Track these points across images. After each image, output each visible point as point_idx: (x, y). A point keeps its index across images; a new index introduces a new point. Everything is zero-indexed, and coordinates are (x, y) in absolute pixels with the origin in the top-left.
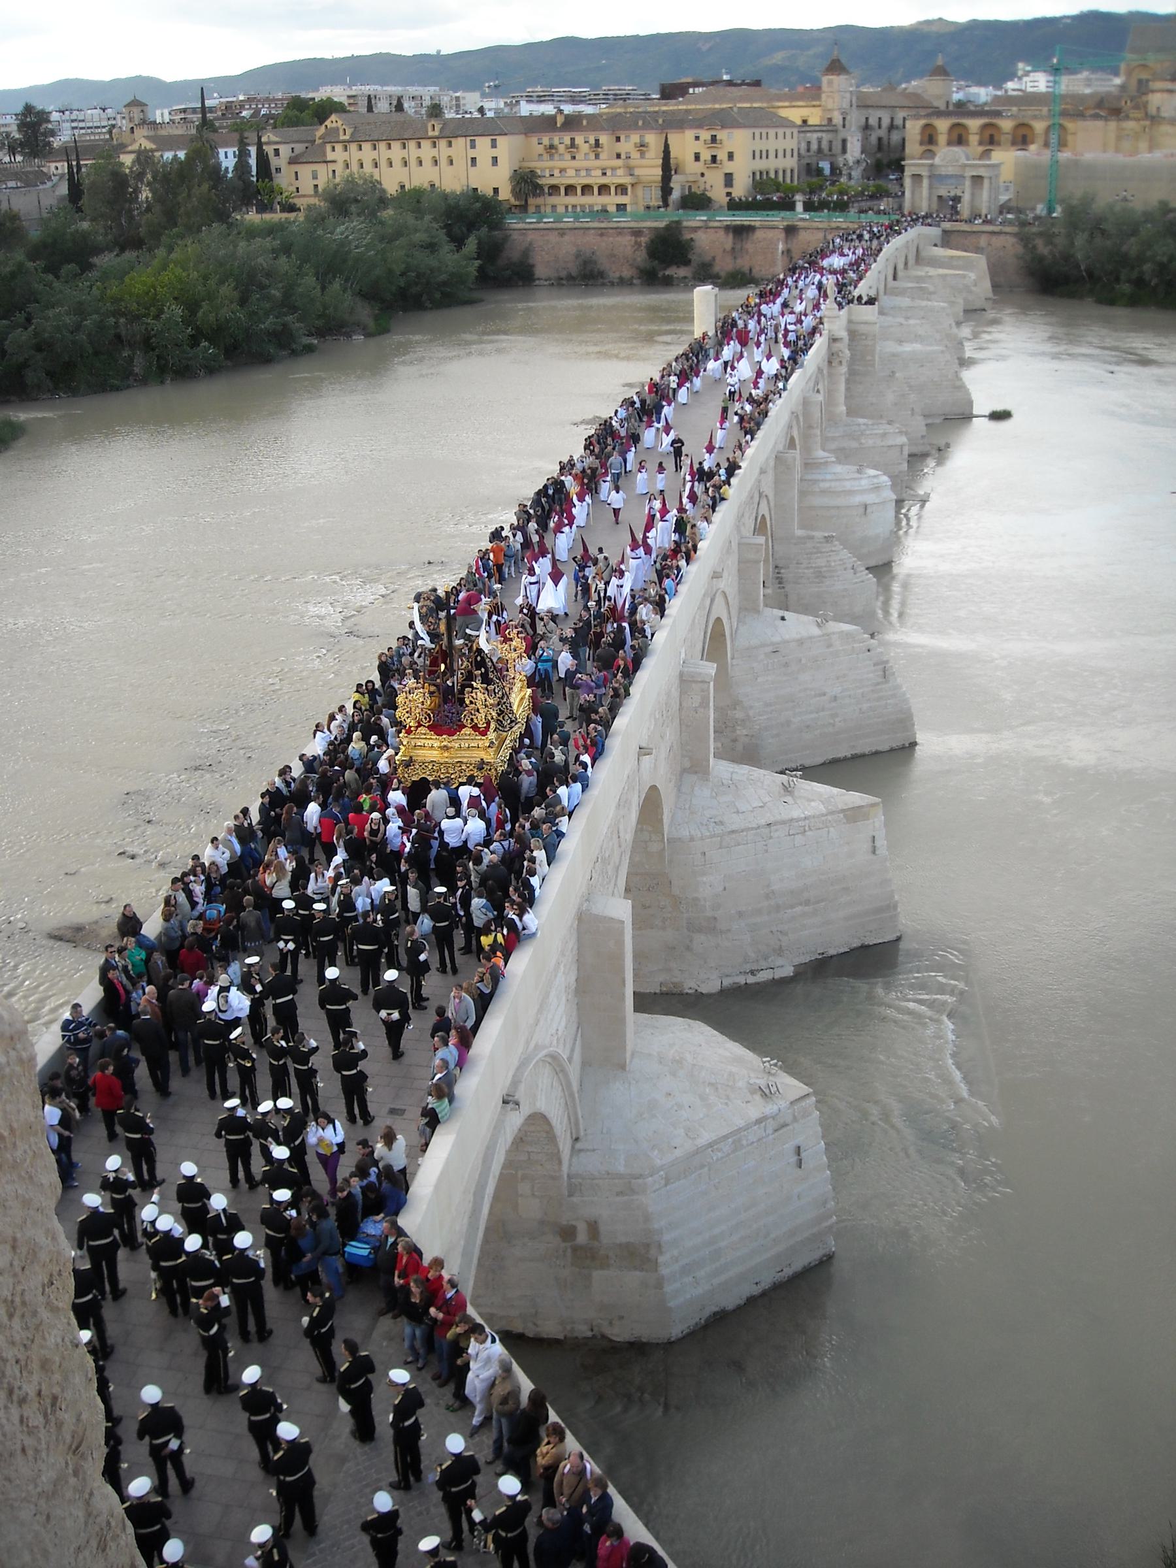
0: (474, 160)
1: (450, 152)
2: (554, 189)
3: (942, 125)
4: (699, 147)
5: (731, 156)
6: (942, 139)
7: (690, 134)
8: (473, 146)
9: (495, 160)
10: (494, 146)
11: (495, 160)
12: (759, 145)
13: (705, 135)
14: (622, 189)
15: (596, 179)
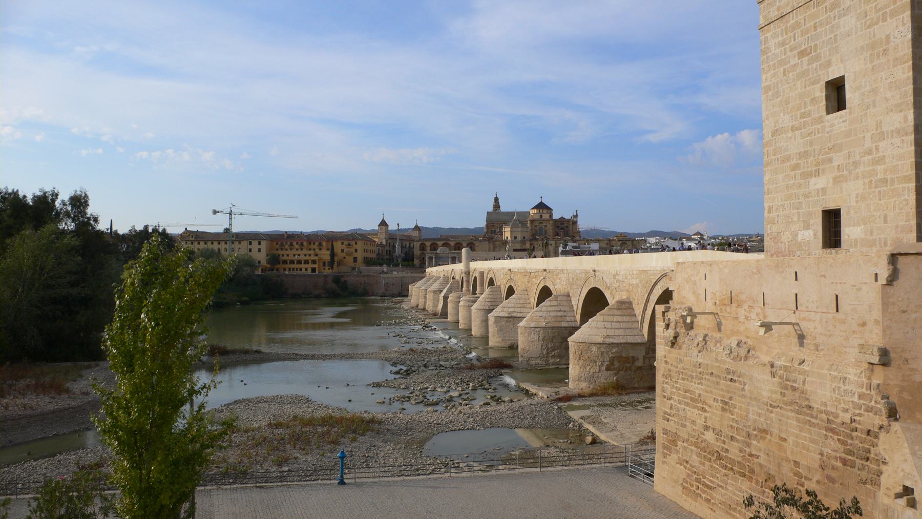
0: (250, 250)
1: (240, 246)
2: (285, 262)
3: (428, 244)
4: (343, 247)
5: (356, 251)
6: (428, 249)
7: (339, 242)
8: (250, 243)
9: (259, 250)
10: (260, 243)
11: (259, 250)
12: (367, 247)
13: (346, 243)
14: (314, 262)
15: (302, 258)
